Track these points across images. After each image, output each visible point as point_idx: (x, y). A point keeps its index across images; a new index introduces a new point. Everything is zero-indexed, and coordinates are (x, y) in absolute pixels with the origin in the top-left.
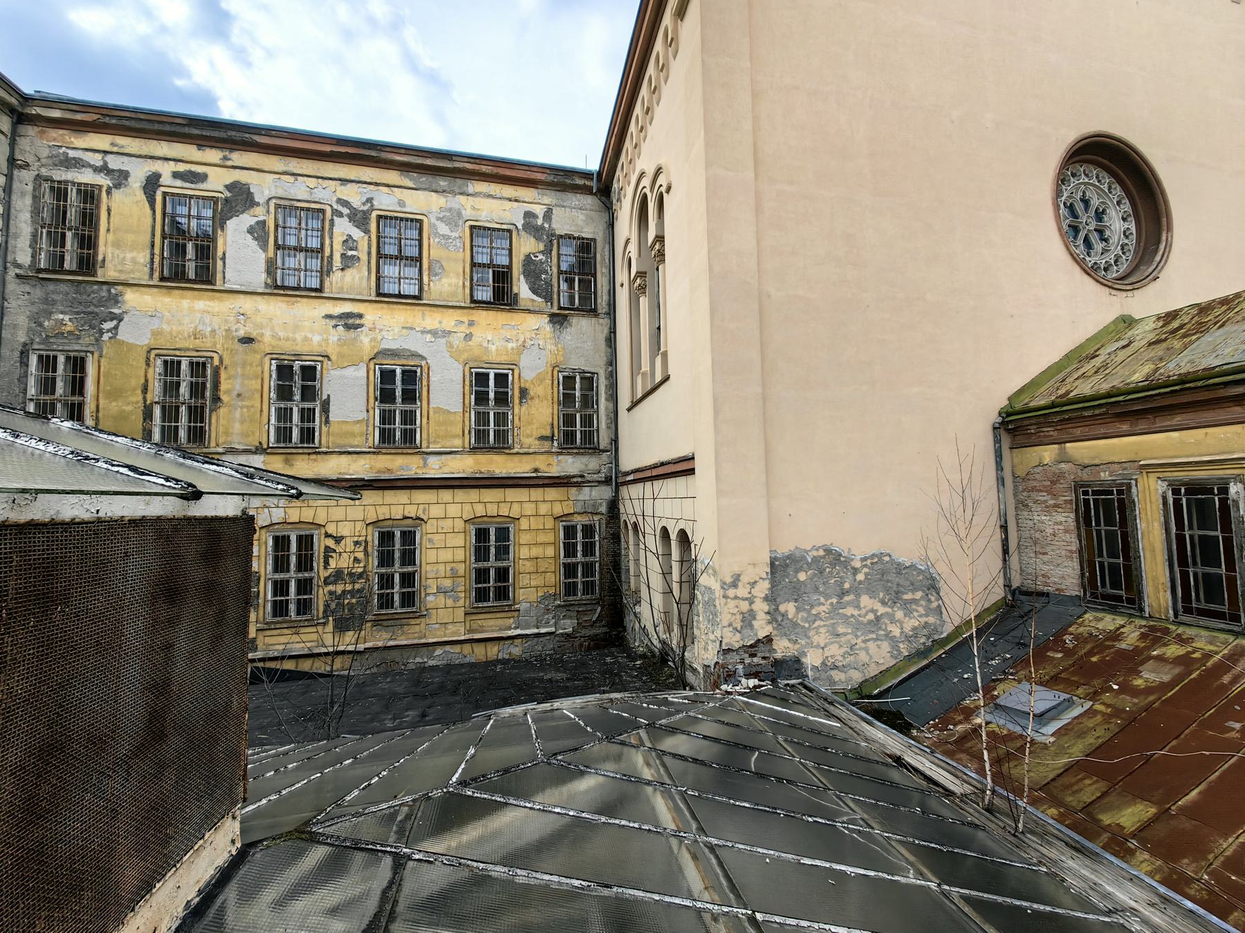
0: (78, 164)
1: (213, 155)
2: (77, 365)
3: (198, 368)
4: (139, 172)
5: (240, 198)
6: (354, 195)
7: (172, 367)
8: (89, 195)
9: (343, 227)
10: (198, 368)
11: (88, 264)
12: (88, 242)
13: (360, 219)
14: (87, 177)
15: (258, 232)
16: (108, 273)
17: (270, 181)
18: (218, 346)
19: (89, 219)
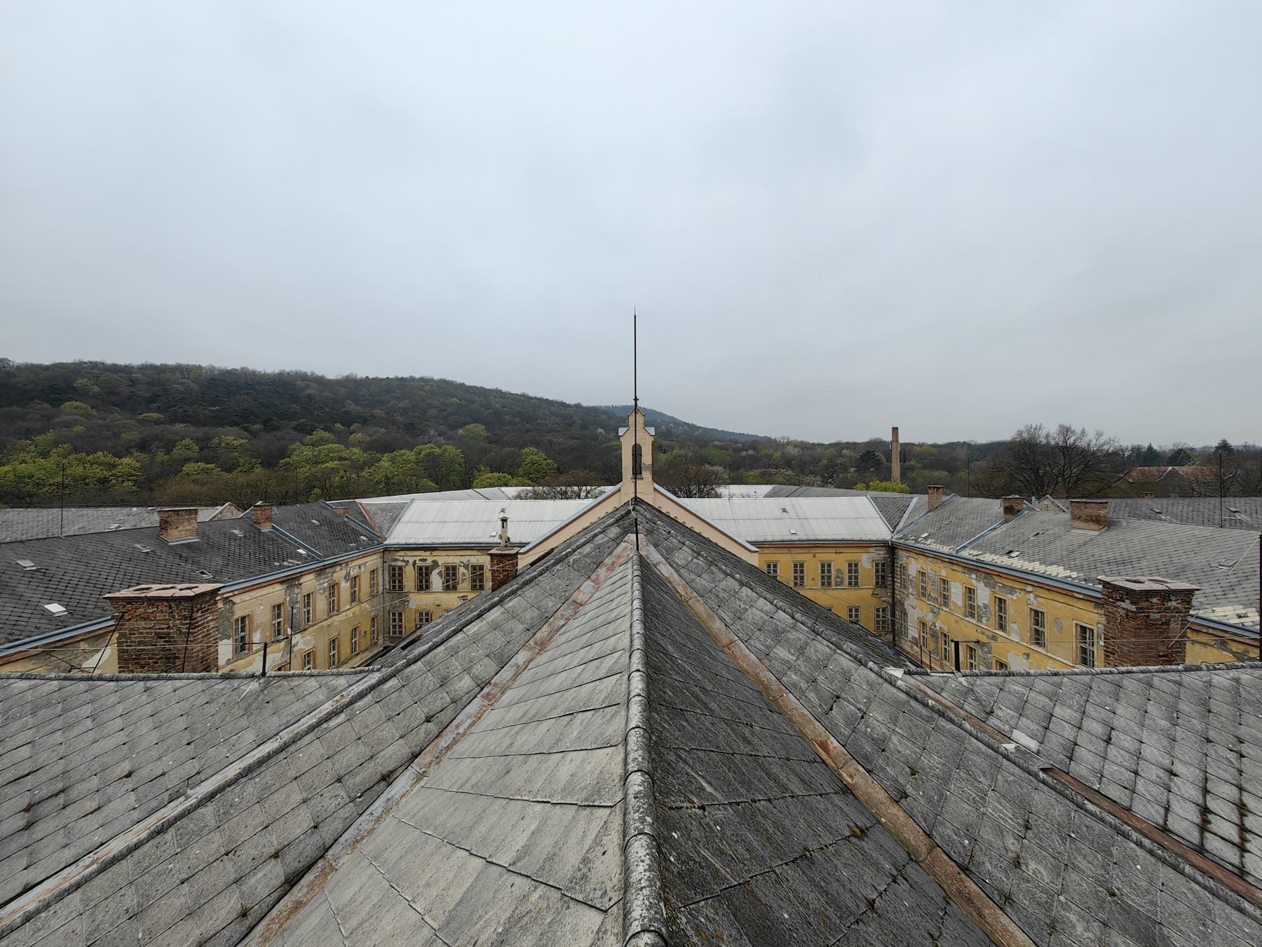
0: (396, 560)
1: (428, 553)
2: (400, 615)
3: (427, 614)
4: (411, 560)
5: (435, 564)
6: (465, 560)
7: (421, 614)
8: (400, 568)
9: (462, 570)
10: (427, 614)
11: (401, 588)
12: (401, 582)
13: (466, 567)
14: (399, 563)
15: (440, 574)
16: (405, 590)
17: (444, 559)
18: (432, 608)
19: (401, 575)
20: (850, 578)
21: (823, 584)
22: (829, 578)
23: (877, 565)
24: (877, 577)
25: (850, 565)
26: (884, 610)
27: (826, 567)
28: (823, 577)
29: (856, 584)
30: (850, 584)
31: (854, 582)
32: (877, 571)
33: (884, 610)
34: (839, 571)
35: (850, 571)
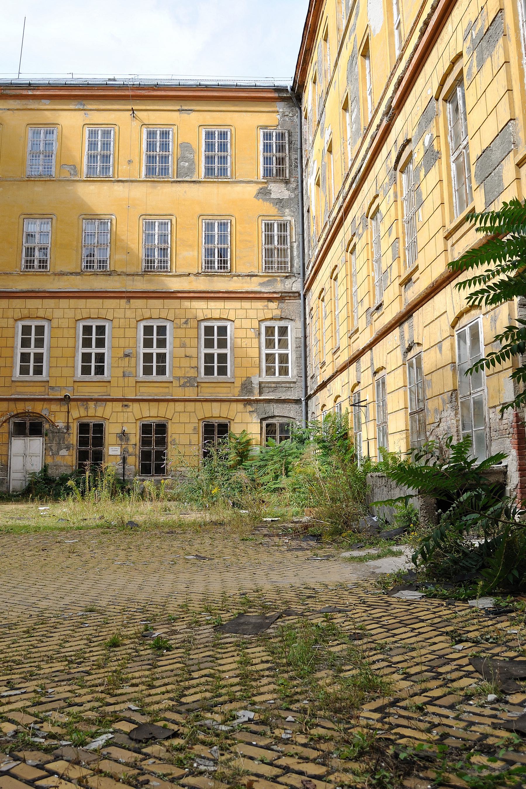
20: (209, 159)
21: (150, 171)
22: (165, 159)
23: (268, 136)
24: (267, 160)
25: (210, 135)
26: (283, 227)
27: (158, 142)
28: (151, 159)
29: (223, 171)
30: (209, 171)
31: (217, 168)
32: (267, 148)
33: (283, 227)
34: (186, 147)
35: (209, 146)
